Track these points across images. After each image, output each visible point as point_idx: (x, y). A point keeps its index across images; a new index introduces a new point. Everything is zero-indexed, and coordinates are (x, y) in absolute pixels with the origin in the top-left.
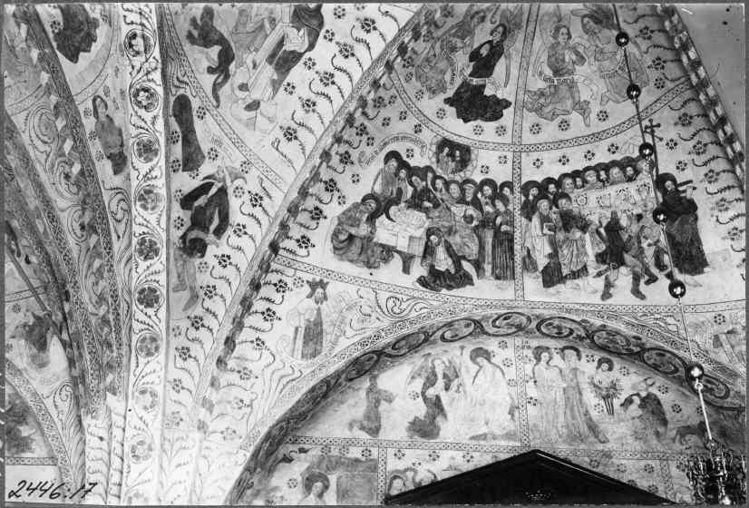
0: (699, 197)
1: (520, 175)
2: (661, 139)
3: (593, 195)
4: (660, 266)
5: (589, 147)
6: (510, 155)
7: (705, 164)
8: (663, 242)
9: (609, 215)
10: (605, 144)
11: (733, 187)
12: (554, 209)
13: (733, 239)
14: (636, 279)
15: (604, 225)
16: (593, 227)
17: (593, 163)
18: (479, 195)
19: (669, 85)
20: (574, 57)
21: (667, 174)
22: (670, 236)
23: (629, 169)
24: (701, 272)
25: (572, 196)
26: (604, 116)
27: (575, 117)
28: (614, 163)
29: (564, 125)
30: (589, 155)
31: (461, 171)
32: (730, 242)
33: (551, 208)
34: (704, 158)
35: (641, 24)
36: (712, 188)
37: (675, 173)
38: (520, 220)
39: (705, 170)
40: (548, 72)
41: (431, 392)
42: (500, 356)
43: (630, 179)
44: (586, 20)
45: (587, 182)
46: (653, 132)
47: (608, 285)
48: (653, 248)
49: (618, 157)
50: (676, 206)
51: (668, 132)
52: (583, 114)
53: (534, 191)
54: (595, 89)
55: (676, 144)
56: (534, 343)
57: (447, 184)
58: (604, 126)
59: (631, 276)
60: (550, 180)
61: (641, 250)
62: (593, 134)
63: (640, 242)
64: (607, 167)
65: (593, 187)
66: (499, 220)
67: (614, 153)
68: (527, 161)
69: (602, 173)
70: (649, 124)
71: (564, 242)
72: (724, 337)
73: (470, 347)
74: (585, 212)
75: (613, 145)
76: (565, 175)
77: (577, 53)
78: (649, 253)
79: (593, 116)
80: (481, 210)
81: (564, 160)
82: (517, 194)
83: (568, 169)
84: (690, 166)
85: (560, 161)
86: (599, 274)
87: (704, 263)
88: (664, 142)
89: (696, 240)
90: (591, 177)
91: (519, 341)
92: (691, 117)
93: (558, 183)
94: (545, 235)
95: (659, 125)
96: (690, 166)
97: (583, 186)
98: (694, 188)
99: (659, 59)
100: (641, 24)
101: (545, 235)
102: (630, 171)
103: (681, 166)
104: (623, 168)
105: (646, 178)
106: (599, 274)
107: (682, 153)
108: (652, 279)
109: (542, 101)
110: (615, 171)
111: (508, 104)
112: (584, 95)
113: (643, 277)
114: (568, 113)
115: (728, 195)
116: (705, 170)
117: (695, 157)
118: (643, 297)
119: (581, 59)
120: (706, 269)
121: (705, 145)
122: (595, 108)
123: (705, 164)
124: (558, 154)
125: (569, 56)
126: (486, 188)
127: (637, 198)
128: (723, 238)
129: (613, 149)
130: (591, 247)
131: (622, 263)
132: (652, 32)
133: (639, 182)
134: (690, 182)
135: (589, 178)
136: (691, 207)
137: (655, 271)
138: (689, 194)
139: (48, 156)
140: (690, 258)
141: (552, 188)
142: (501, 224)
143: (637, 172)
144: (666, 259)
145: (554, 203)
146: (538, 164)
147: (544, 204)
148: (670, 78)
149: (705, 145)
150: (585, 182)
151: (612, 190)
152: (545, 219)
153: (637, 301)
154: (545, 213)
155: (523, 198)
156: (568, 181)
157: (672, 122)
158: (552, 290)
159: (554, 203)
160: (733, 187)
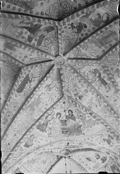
139: (16, 128)
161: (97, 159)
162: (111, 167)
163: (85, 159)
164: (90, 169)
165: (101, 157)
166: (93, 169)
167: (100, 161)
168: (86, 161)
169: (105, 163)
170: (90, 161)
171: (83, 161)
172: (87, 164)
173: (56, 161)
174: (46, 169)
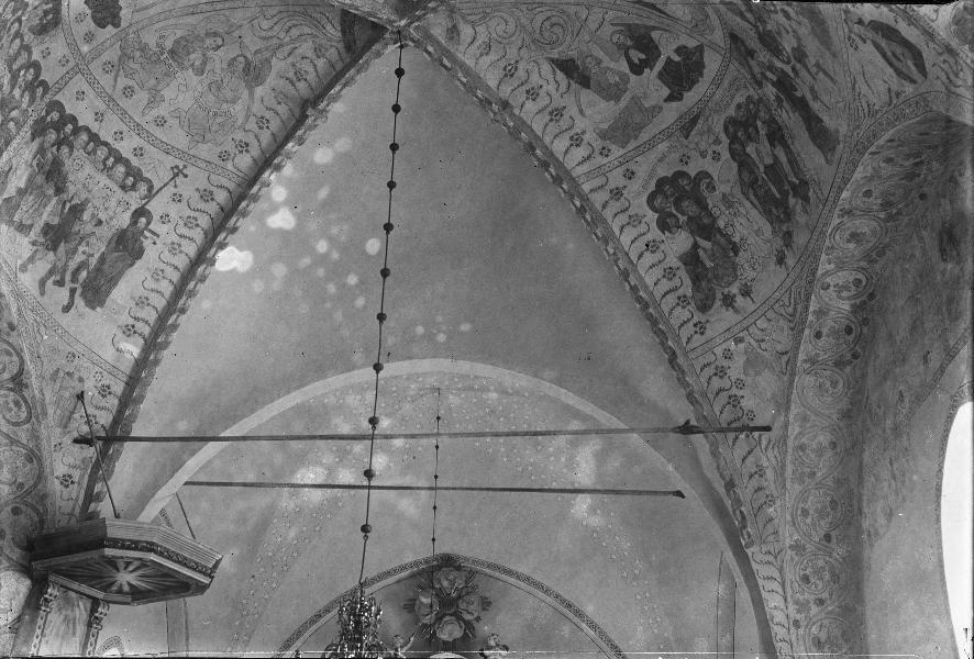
0: (151, 252)
1: (60, 89)
2: (176, 186)
3: (88, 169)
4: (74, 279)
5: (125, 128)
6: (71, 64)
7: (181, 236)
8: (93, 261)
9: (83, 196)
10: (137, 142)
11: (179, 270)
12: (54, 149)
13: (137, 304)
14: (51, 273)
15: (73, 203)
16: (64, 196)
17: (116, 145)
18: (22, 72)
19: (229, 166)
20: (197, 63)
21: (150, 212)
22: (102, 259)
23: (131, 179)
24: (93, 308)
25: (76, 153)
26: (161, 122)
27: (142, 96)
28: (127, 163)
29: (128, 92)
30: (119, 135)
31: (34, 33)
32: (133, 304)
33: (53, 145)
34: (184, 231)
35: (268, 115)
36: (167, 256)
37: (156, 217)
38: (26, 131)
39: (176, 239)
40: (169, 44)
43: (123, 187)
44: (241, 59)
45: (95, 154)
46: (177, 175)
48: (84, 257)
49: (135, 162)
50: (128, 245)
51: (186, 188)
52: (150, 102)
53: (55, 116)
54: (181, 98)
55: (179, 201)
57: (18, 35)
58: (152, 128)
59: (50, 266)
60: (73, 119)
61: (74, 251)
62: (138, 125)
63: (80, 244)
64: (119, 159)
65: (94, 162)
66: (14, 114)
67: (135, 155)
68: (79, 83)
69: (112, 159)
70: (181, 167)
71: (38, 187)
72: (62, 374)
74: (71, 177)
75: (141, 149)
76: (87, 129)
77: (204, 63)
78: (79, 258)
79: (155, 113)
80: (13, 87)
81: (99, 117)
82: (43, 105)
83: (95, 127)
84: (171, 225)
85: (96, 114)
87: (102, 303)
88: (174, 191)
89: (113, 281)
90: (102, 152)
92: (212, 199)
93: (77, 131)
94: (31, 166)
95: (186, 176)
96: (171, 225)
97: (89, 153)
98: (154, 243)
99: (247, 145)
100: (268, 115)
101: (31, 166)
102: (130, 180)
103: (165, 218)
104: (128, 174)
105: (135, 200)
107: (174, 211)
108: (60, 283)
109: (138, 54)
110: (121, 169)
111: (116, 25)
112: (168, 93)
113: (57, 276)
114: (142, 88)
115: (169, 270)
116: (176, 239)
117: (181, 223)
119: (200, 72)
120: (98, 309)
121: (197, 225)
122: (162, 110)
123: (181, 236)
124: (101, 106)
125: (196, 57)
126: (32, 70)
127: (113, 203)
128: (132, 298)
129: (139, 152)
130: (49, 214)
131: (55, 249)
132: (268, 127)
133: (127, 197)
134: (158, 236)
135: (99, 152)
136: (139, 253)
137: (68, 277)
138: (147, 243)
140: (95, 290)
141: (70, 127)
142: (12, 119)
143: (133, 187)
144: (84, 274)
145: (59, 144)
146: (81, 95)
147: (52, 136)
148: (236, 161)
149: (197, 225)
150: (94, 151)
151: (104, 180)
152: (41, 151)
154: (47, 145)
155: (44, 113)
156: (84, 137)
157: (197, 186)
159: (59, 144)
160: (179, 270)
161: (637, 69)
162: (726, 129)
163: (546, 68)
164: (577, 141)
165: (668, 51)
166: (598, 144)
167: (651, 86)
168: (551, 88)
169: (691, 97)
170: (585, 82)
171: (535, 79)
172: (558, 102)
173: (339, 66)
174: (262, 122)
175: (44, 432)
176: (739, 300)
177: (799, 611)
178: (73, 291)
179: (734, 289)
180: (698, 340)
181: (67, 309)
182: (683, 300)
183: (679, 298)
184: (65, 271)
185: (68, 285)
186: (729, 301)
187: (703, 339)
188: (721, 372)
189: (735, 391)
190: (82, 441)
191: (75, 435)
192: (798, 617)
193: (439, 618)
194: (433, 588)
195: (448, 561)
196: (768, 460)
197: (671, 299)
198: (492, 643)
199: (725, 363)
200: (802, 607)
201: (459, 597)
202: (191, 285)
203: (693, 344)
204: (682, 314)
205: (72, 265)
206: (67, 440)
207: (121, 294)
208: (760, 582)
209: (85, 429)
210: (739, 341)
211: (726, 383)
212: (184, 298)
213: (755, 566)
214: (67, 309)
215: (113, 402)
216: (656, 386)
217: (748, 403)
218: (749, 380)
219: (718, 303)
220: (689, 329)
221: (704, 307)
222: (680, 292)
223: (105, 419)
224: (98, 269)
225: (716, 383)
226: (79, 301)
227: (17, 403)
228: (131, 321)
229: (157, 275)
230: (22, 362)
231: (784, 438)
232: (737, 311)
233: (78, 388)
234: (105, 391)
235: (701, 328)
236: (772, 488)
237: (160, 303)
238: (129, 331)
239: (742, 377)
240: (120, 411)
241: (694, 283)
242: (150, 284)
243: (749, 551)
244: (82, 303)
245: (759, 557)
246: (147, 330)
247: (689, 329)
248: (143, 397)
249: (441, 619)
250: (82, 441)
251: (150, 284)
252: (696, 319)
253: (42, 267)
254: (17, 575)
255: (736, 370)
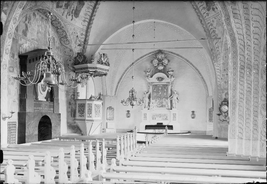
4: (72, 13)
14: (67, 13)
22: (77, 7)
41: (27, 22)
42: (38, 17)
47: (64, 12)
56: (42, 16)
73: (33, 12)
78: (72, 8)
86: (63, 9)
89: (80, 11)
91: (41, 14)
106: (63, 9)
118: (67, 18)
131: (67, 9)
137: (71, 13)
153: (66, 18)
158: (57, 9)
175: (72, 45)
176: (216, 9)
177: (222, 76)
178: (72, 16)
179: (214, 7)
180: (207, 17)
181: (72, 20)
182: (204, 8)
183: (203, 7)
184: (70, 13)
185: (71, 15)
186: (213, 9)
187: (208, 17)
188: (212, 25)
189: (214, 29)
190: (79, 45)
191: (78, 44)
192: (222, 77)
193: (158, 64)
194: (157, 58)
195: (160, 52)
196: (219, 45)
197: (201, 8)
198: (170, 70)
199: (213, 23)
200: (223, 75)
201: (163, 60)
202: (96, 10)
203: (206, 18)
204: (204, 11)
205: (71, 10)
206: (77, 46)
207: (82, 13)
208: (216, 70)
209: (79, 43)
210: (215, 18)
211: (212, 27)
212: (94, 13)
213: (215, 67)
214: (72, 20)
215: (84, 36)
216: (198, 26)
217: (217, 32)
218: (217, 28)
219: (211, 9)
220: (205, 15)
221: (209, 10)
222: (203, 6)
223: (83, 40)
224: (76, 10)
225: (211, 27)
226: (74, 17)
227: (66, 41)
228: (85, 19)
229: (88, 8)
230: (66, 33)
231: (222, 42)
232: (215, 12)
233: (77, 35)
234: (82, 34)
235: (208, 14)
236: (220, 51)
237: (90, 14)
238: (84, 21)
239: (216, 26)
240: (86, 39)
241: (206, 4)
242: (87, 10)
243: (214, 64)
244: (74, 17)
245: (216, 65)
246: (88, 20)
247: (205, 15)
248: (89, 35)
249: (159, 65)
250: (79, 45)
251: (87, 10)
252: (207, 13)
253: (66, 13)
254: (73, 72)
255: (215, 25)
